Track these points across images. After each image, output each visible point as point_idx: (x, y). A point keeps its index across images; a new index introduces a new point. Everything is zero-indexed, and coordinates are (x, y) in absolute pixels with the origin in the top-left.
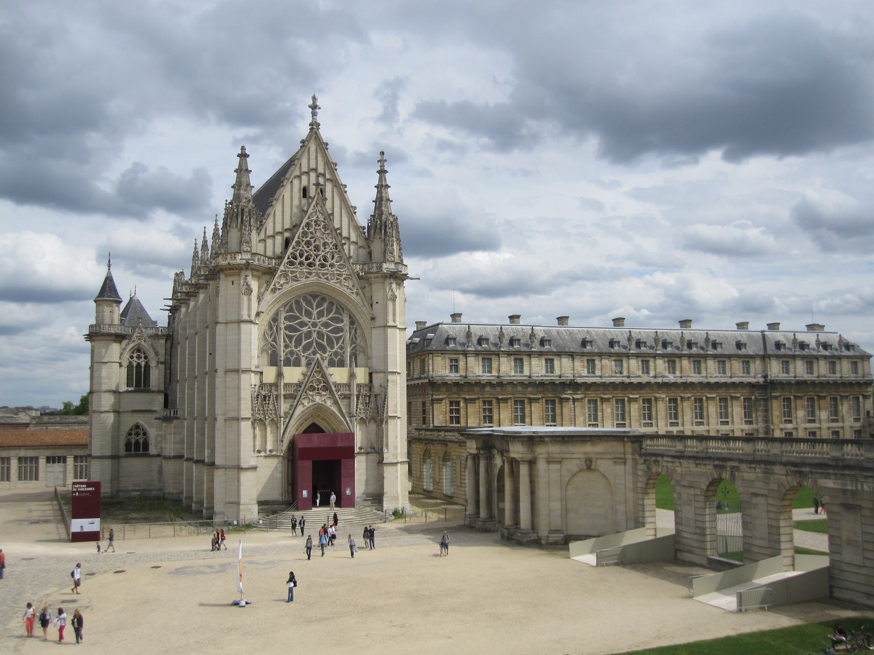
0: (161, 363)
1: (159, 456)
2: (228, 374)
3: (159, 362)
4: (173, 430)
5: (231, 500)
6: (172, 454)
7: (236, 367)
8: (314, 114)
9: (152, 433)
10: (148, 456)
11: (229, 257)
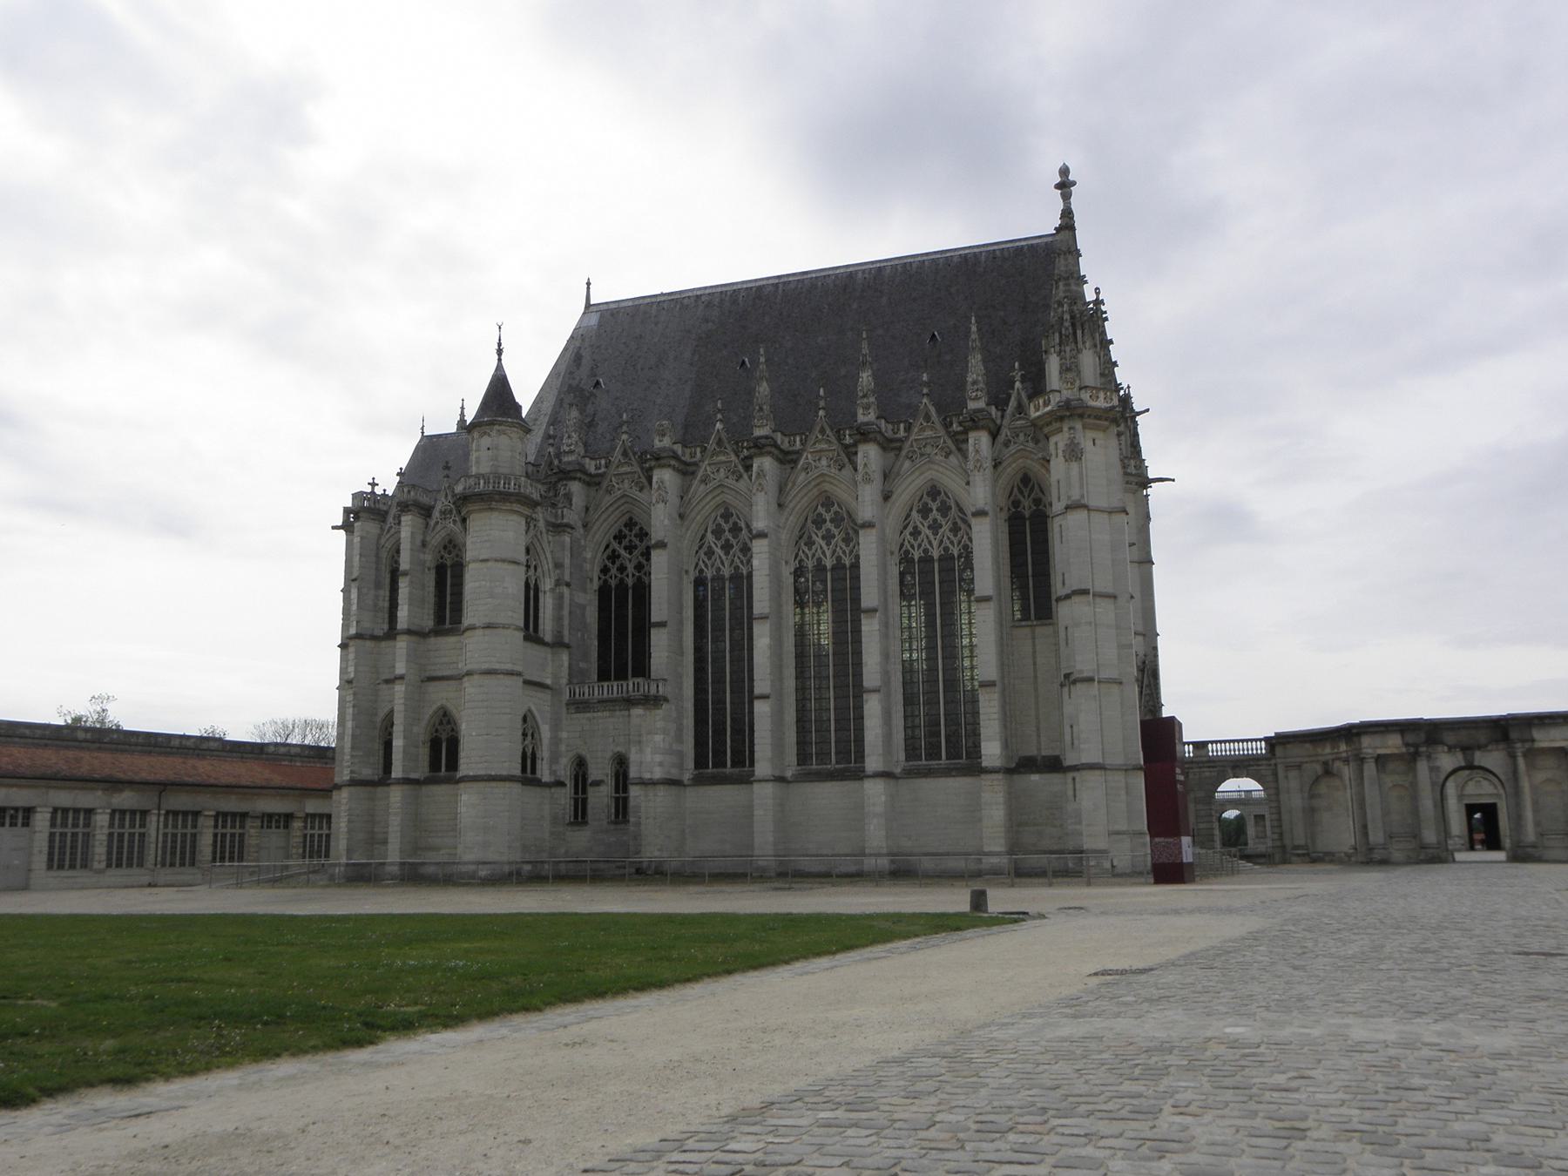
0: (568, 585)
1: (560, 784)
2: (1098, 600)
3: (558, 583)
4: (660, 724)
5: (1117, 827)
6: (658, 774)
7: (1110, 590)
8: (1066, 197)
9: (545, 732)
10: (537, 783)
11: (1102, 395)
